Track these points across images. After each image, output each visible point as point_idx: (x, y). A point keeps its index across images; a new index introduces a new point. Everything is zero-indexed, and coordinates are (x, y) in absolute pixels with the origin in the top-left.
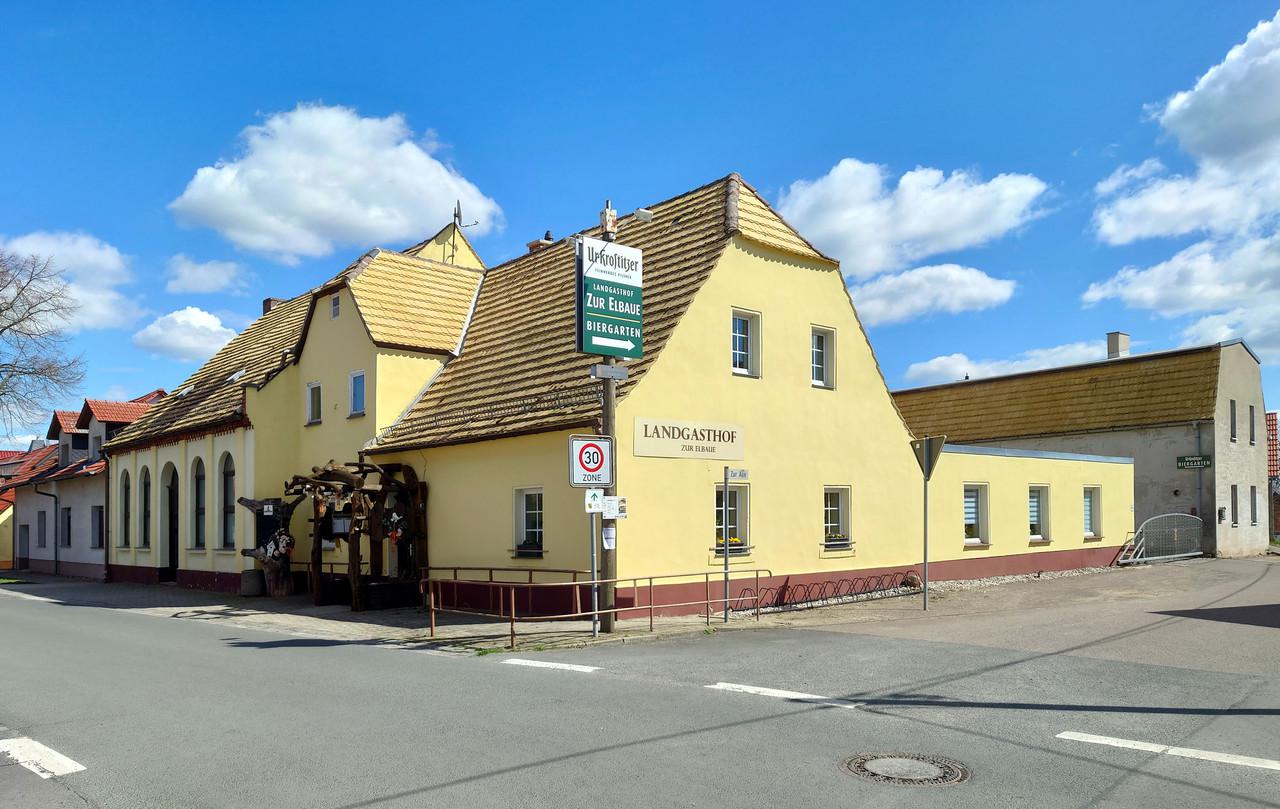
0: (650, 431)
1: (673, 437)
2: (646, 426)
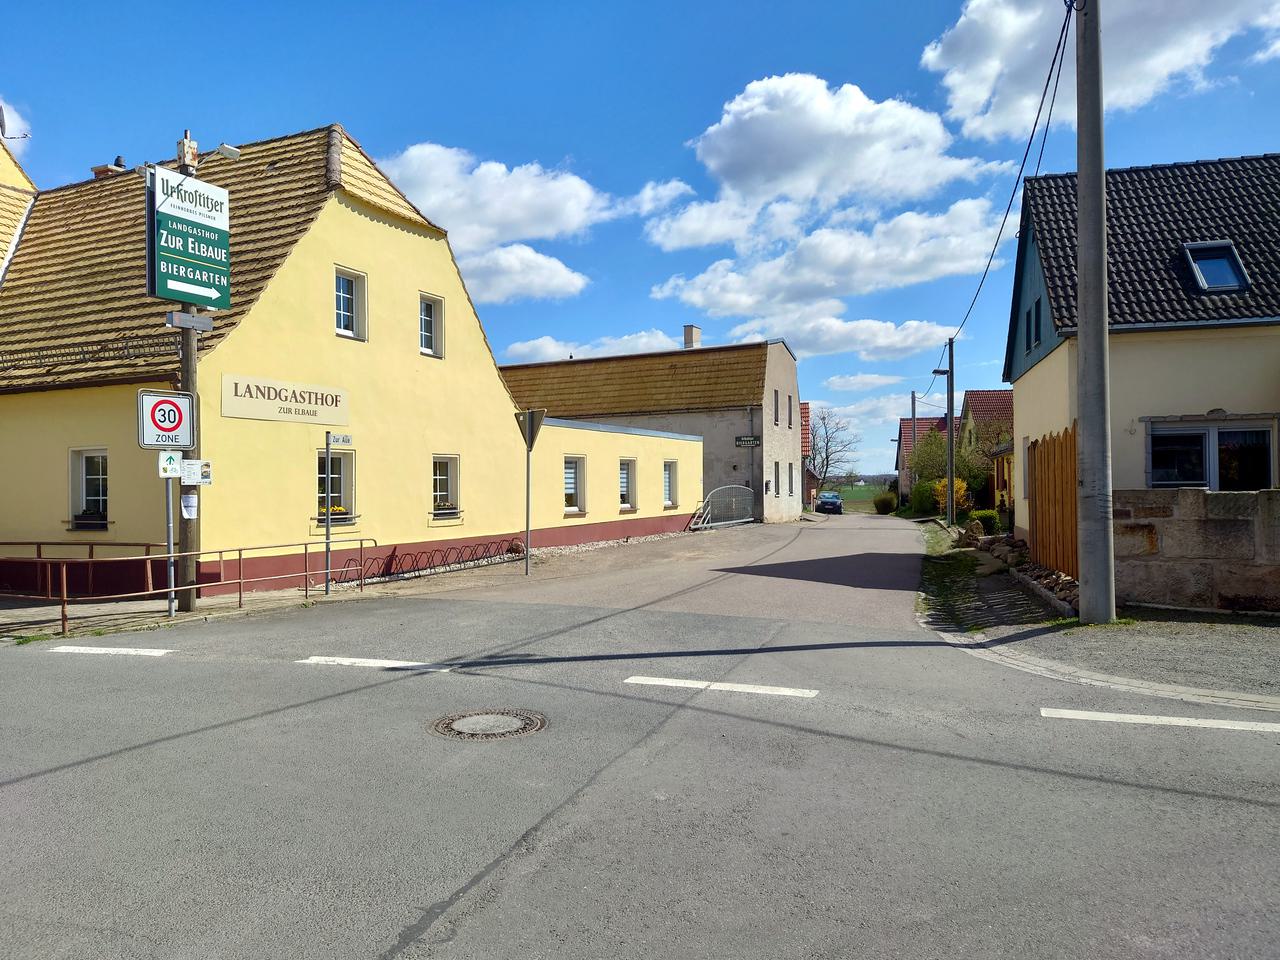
0: (242, 390)
2: (236, 384)
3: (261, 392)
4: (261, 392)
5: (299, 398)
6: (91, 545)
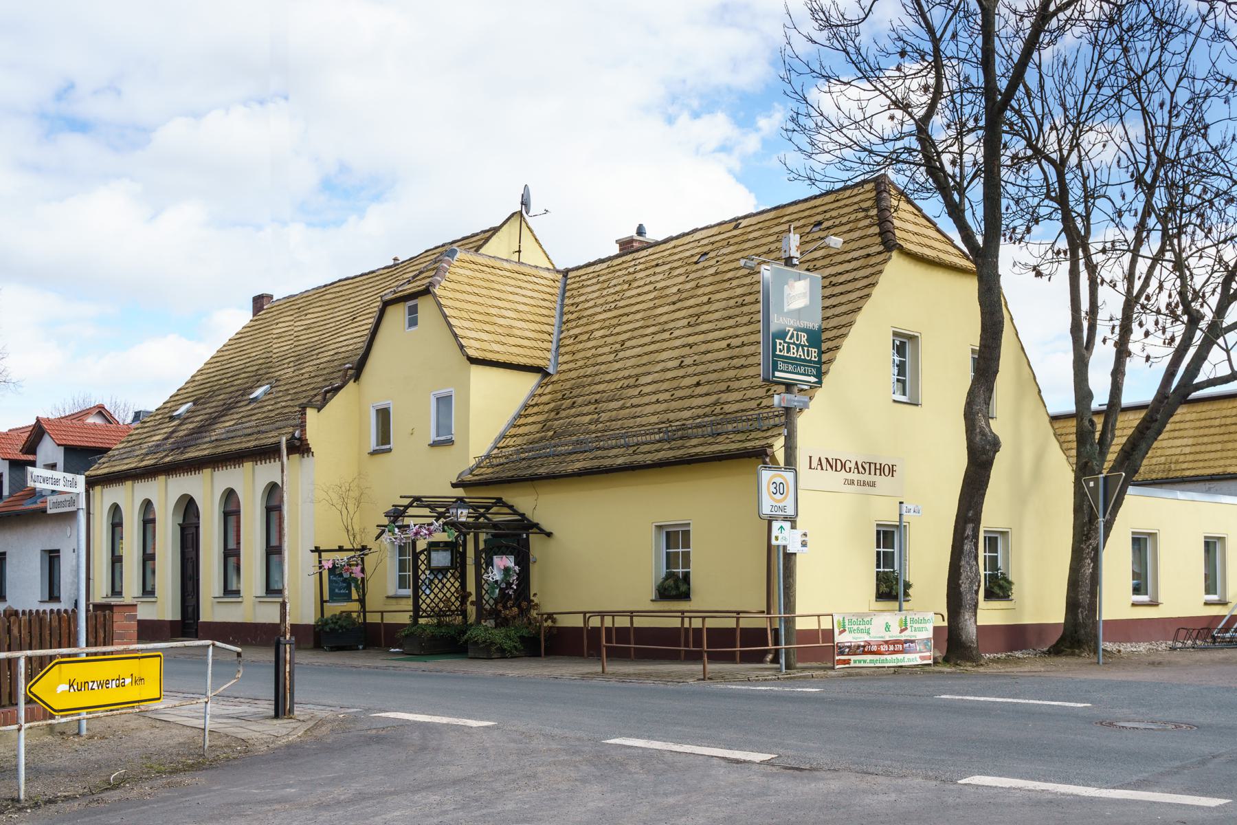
0: (815, 463)
1: (836, 470)
2: (810, 457)
5: (861, 469)
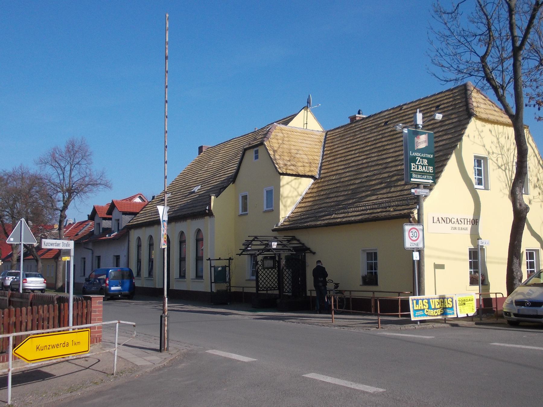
0: (436, 220)
1: (447, 223)
2: (433, 217)
3: (443, 220)
4: (443, 220)
5: (460, 222)
6: (374, 292)
